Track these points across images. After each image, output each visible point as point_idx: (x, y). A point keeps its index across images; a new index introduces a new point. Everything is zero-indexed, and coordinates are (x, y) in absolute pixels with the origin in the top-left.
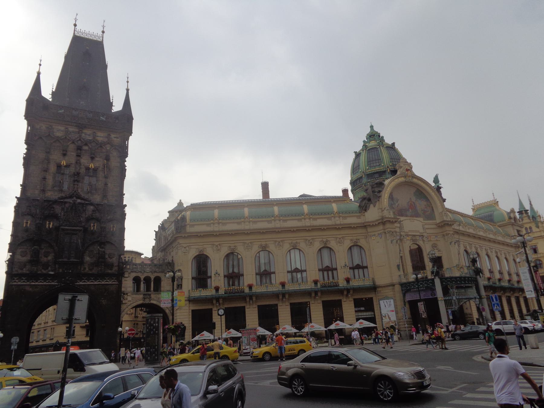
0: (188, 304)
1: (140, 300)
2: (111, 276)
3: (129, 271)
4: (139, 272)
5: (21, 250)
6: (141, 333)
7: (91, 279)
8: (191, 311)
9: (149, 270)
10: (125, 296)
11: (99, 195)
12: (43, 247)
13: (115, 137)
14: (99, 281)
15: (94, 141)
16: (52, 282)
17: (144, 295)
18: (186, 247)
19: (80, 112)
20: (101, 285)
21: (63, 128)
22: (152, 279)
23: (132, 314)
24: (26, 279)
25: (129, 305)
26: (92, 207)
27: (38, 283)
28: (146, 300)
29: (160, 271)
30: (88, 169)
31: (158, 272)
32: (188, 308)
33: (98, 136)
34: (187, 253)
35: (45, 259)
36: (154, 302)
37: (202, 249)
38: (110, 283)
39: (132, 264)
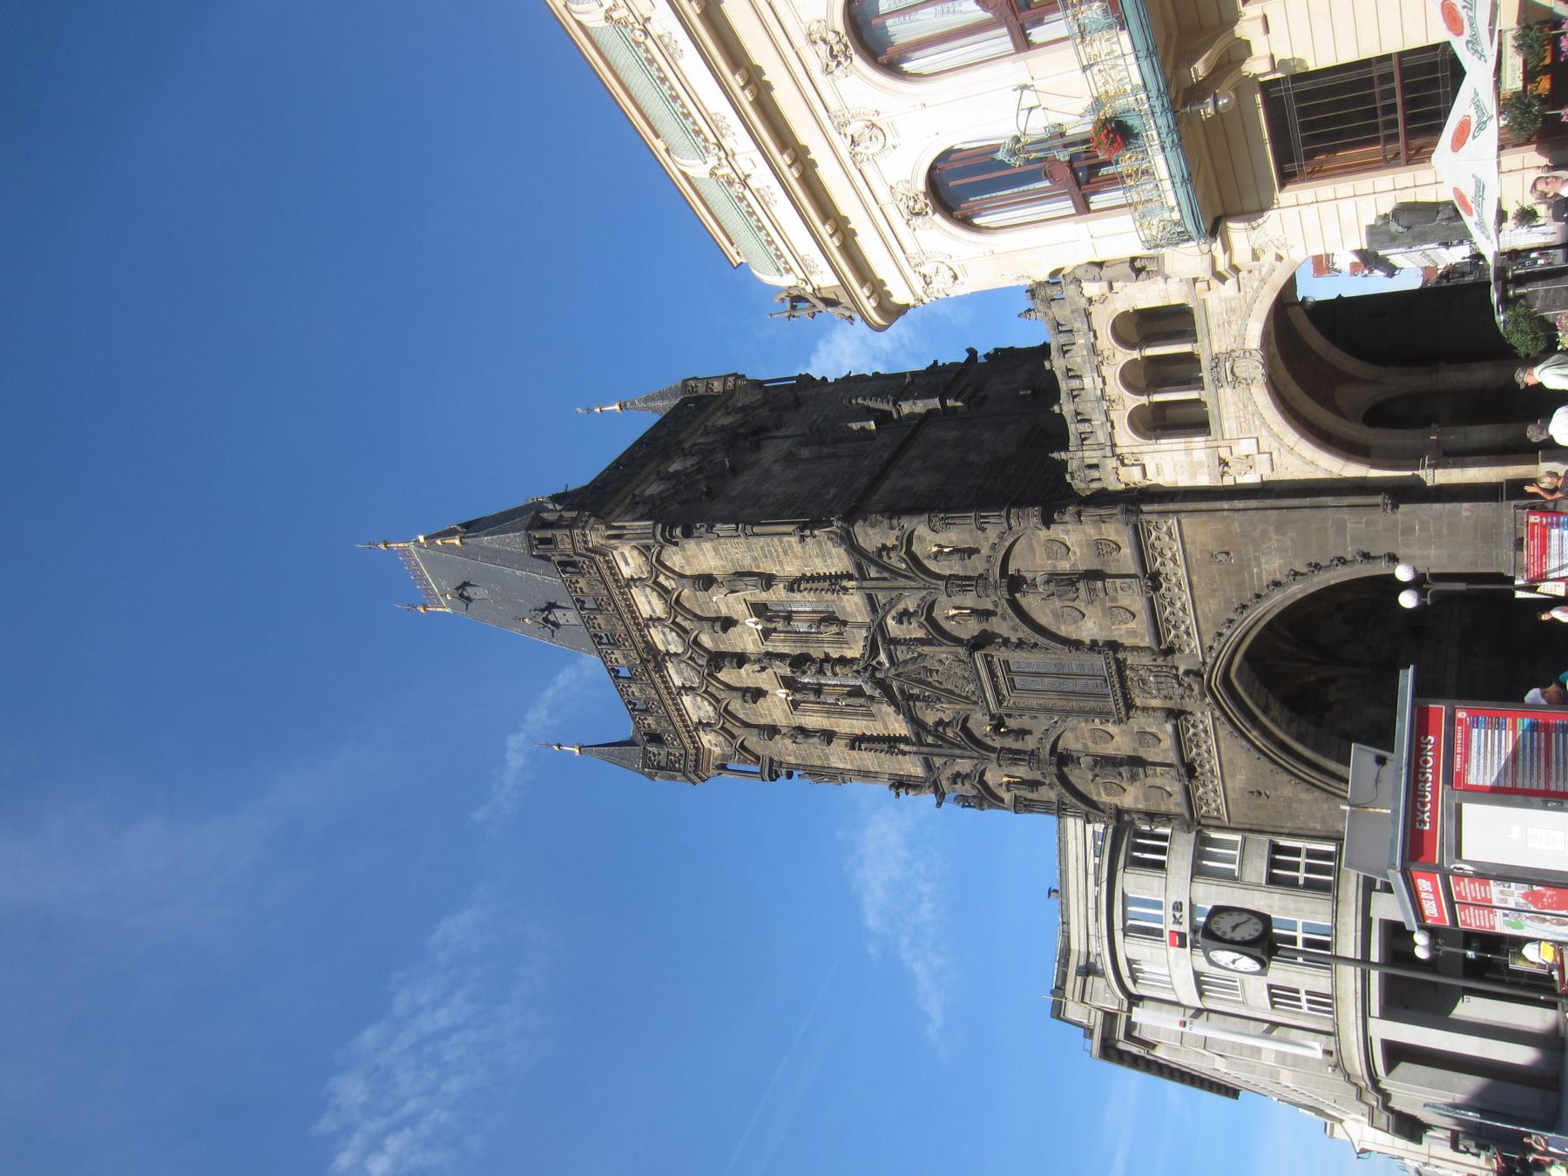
4: (1108, 419)
5: (1103, 794)
11: (841, 599)
13: (627, 564)
14: (1179, 585)
15: (674, 622)
17: (1218, 383)
18: (925, 276)
19: (611, 661)
20: (1195, 579)
21: (687, 700)
26: (890, 622)
28: (1244, 375)
29: (1087, 327)
30: (766, 634)
31: (1091, 333)
33: (654, 611)
34: (950, 269)
35: (1116, 738)
37: (902, 206)
38: (1177, 546)
39: (1080, 454)
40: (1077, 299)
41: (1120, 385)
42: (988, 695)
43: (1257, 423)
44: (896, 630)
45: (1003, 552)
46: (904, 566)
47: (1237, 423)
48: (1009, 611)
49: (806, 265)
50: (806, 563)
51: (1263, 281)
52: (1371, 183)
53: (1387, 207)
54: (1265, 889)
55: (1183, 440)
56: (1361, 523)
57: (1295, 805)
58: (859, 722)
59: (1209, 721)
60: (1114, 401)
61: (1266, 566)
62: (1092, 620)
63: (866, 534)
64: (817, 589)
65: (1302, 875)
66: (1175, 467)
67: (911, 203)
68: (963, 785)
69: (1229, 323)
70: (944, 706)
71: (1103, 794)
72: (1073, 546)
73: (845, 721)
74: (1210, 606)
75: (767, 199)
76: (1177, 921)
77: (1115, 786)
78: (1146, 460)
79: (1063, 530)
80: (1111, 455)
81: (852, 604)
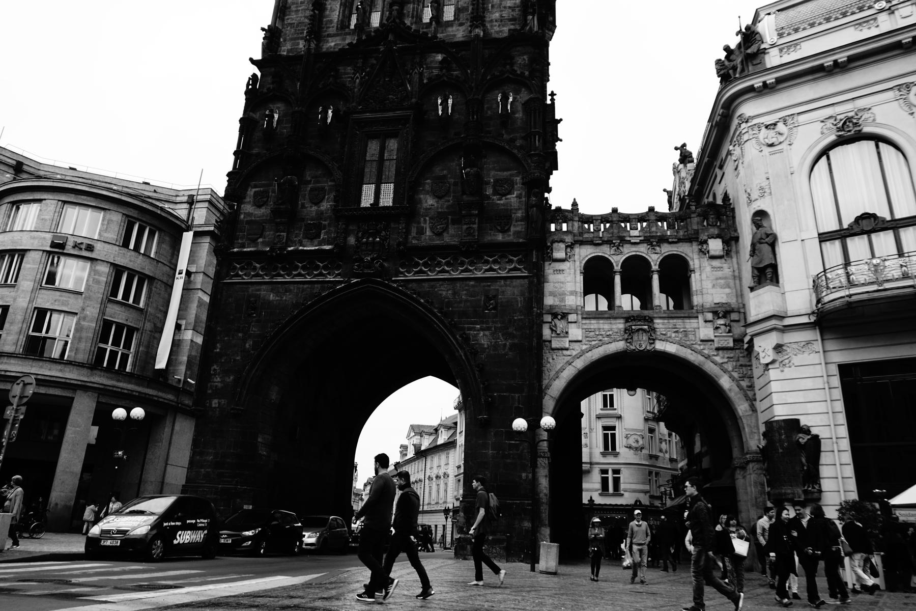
0: (818, 346)
1: (615, 341)
2: (502, 251)
3: (567, 240)
4: (604, 242)
5: (254, 190)
6: (668, 497)
7: (439, 264)
8: (834, 370)
9: (638, 235)
10: (561, 325)
11: (461, 25)
12: (309, 179)
16: (329, 274)
18: (775, 124)
22: (655, 267)
23: (642, 448)
24: (262, 269)
25: (578, 356)
27: (293, 278)
28: (635, 337)
29: (681, 237)
32: (818, 358)
35: (314, 208)
36: (671, 348)
37: (852, 114)
38: (503, 274)
39: (577, 219)
40: (706, 234)
41: (630, 254)
42: (368, 114)
43: (593, 343)
44: (432, 59)
45: (507, 147)
46: (497, 73)
47: (595, 329)
48: (450, 143)
49: (791, 46)
50: (496, 6)
51: (708, 357)
52: (842, 423)
53: (814, 431)
54: (100, 317)
55: (582, 291)
56: (519, 404)
57: (240, 335)
58: (337, 16)
59: (330, 278)
60: (618, 248)
61: (482, 334)
62: (435, 204)
63: (524, 54)
64: (478, 5)
65: (109, 347)
66: (562, 283)
67: (855, 121)
68: (273, 83)
69: (676, 332)
70: (358, 81)
71: (257, 189)
72: (506, 199)
73: (338, 7)
74: (445, 292)
75: (865, 25)
76: (76, 246)
77: (265, 199)
78: (565, 266)
79: (521, 194)
80: (576, 239)
81: (459, 33)
